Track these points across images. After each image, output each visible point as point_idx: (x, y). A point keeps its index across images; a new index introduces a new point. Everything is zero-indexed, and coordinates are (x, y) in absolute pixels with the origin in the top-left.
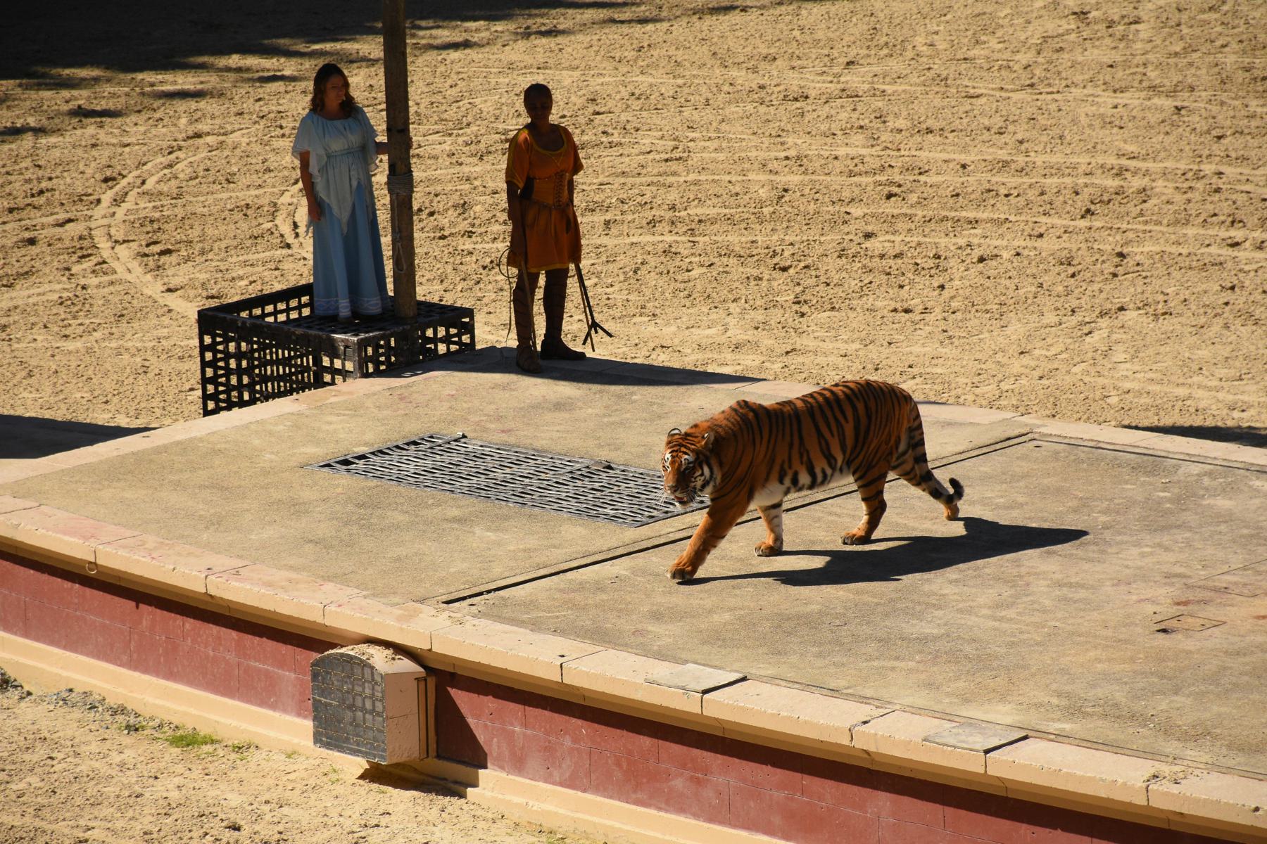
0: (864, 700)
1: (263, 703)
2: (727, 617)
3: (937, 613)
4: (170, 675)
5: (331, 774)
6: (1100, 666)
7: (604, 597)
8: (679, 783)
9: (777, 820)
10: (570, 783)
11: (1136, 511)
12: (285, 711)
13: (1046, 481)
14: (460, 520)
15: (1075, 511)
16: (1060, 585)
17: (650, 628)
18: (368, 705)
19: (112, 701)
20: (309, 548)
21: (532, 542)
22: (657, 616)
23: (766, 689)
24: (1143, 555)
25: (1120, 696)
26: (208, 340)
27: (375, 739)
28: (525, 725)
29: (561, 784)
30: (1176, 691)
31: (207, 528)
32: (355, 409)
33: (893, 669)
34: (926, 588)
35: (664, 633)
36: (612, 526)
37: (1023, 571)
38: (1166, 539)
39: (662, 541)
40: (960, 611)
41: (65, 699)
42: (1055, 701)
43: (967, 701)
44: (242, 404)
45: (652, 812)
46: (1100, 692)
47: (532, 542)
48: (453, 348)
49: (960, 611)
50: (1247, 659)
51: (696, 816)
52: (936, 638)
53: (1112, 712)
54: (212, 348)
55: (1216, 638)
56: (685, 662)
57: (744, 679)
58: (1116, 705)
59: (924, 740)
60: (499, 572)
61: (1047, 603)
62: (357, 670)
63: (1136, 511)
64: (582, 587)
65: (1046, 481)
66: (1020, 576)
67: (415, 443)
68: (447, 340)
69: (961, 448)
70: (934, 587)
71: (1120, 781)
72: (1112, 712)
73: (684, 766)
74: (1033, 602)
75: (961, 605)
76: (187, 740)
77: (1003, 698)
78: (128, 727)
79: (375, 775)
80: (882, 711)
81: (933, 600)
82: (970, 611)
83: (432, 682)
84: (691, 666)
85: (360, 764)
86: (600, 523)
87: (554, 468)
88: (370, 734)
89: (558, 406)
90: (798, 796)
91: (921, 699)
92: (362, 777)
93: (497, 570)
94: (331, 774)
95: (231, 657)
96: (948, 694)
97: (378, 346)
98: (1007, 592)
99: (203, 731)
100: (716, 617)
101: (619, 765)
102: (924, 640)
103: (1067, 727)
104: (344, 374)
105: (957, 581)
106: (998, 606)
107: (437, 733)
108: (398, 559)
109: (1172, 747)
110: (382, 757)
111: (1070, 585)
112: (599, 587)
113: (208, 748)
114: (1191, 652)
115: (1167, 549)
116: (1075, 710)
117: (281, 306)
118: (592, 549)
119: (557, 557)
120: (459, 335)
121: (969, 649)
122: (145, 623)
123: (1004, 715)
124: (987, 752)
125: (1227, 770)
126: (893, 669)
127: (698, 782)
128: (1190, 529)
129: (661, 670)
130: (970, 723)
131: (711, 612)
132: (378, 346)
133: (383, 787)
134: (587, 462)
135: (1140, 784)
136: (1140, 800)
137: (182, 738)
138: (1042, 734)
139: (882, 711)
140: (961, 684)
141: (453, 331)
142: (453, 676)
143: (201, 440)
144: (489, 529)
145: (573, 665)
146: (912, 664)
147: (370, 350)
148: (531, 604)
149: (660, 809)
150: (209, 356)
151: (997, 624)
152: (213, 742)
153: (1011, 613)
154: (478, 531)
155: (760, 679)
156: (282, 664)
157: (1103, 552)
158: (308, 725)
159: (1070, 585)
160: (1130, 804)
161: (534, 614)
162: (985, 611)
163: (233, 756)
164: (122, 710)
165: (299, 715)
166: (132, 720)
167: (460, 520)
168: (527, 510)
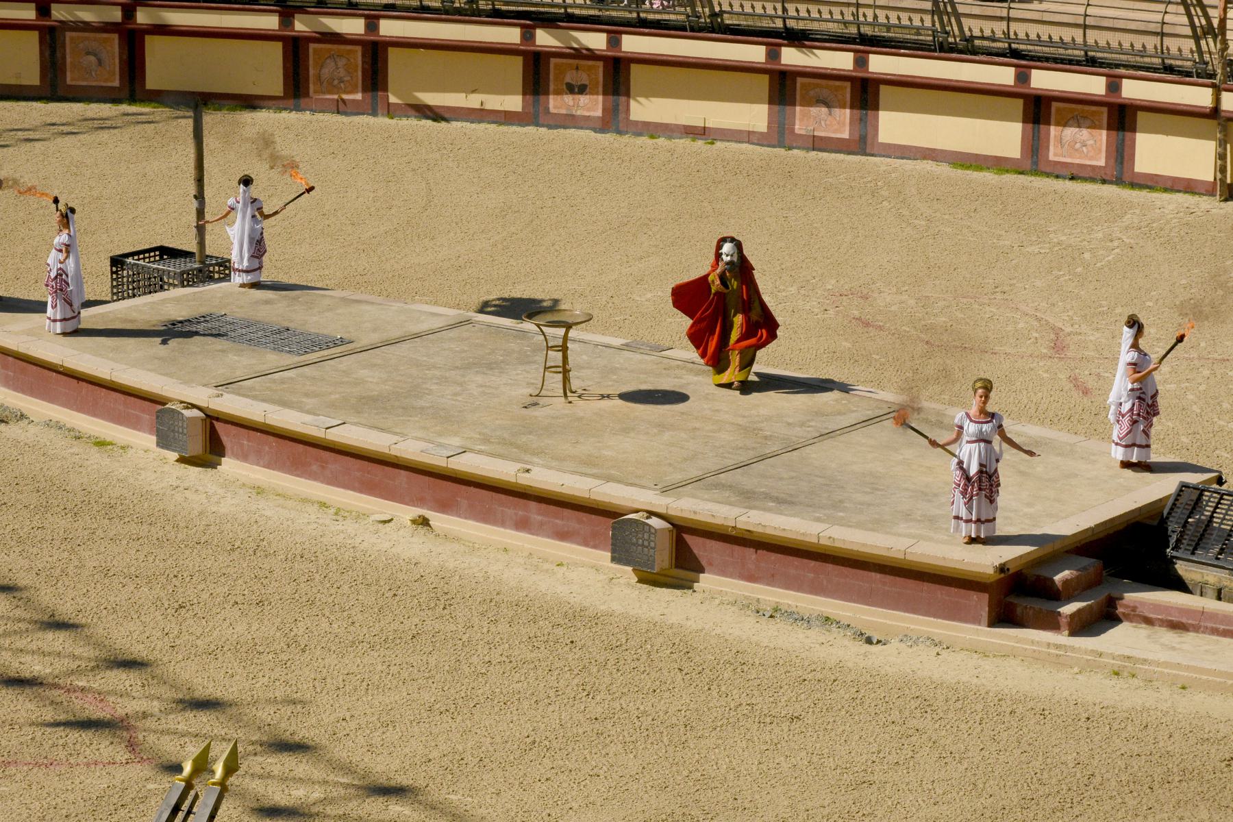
0: (396, 434)
1: (135, 428)
2: (337, 396)
3: (430, 397)
4: (95, 415)
5: (164, 460)
6: (497, 422)
7: (285, 386)
8: (314, 468)
9: (357, 485)
10: (268, 466)
11: (515, 355)
12: (145, 432)
13: (477, 341)
14: (223, 351)
15: (489, 354)
16: (482, 386)
17: (304, 400)
18: (181, 430)
19: (68, 426)
20: (156, 361)
21: (254, 361)
22: (307, 395)
23: (354, 428)
24: (517, 374)
25: (506, 435)
26: (114, 269)
27: (183, 445)
28: (249, 441)
29: (263, 467)
30: (530, 433)
31: (112, 351)
32: (177, 300)
33: (409, 421)
34: (424, 386)
35: (310, 402)
36: (288, 355)
37: (466, 379)
38: (528, 367)
39: (310, 362)
40: (438, 396)
41: (49, 424)
42: (478, 436)
43: (441, 435)
44: (129, 297)
45: (303, 480)
46: (498, 433)
47: (254, 361)
48: (222, 276)
49: (438, 396)
50: (561, 421)
51: (322, 482)
52: (428, 408)
53: (503, 442)
54: (116, 273)
55: (547, 411)
56: (319, 415)
57: (344, 423)
58: (504, 439)
59: (422, 452)
60: (239, 374)
61: (475, 393)
62: (176, 415)
63: (515, 355)
64: (274, 381)
65: (477, 341)
66: (464, 382)
67: (204, 317)
68: (219, 272)
69: (441, 326)
70: (428, 386)
71: (505, 471)
72: (503, 442)
73: (317, 460)
74: (470, 394)
75: (439, 394)
76: (101, 444)
77: (456, 434)
78: (75, 437)
79: (182, 460)
80: (403, 439)
81: (427, 392)
82: (442, 396)
83: (208, 421)
84: (321, 417)
85: (175, 456)
86: (283, 354)
87: (264, 330)
88: (181, 443)
89: (267, 302)
90: (366, 475)
91: (420, 434)
92: (177, 461)
93: (238, 373)
94: (164, 460)
95: (121, 408)
96: (432, 433)
97: (189, 274)
98: (459, 389)
99: (108, 439)
100: (333, 397)
101: (288, 458)
102: (422, 408)
103: (483, 448)
104: (175, 286)
105: (437, 383)
106: (456, 394)
107: (210, 443)
108: (195, 367)
109: (527, 457)
110: (186, 453)
111: (485, 386)
112: (283, 382)
113: (109, 447)
114: (536, 417)
115: (528, 372)
116: (486, 440)
117: (147, 255)
118: (279, 365)
119: (264, 368)
120: (224, 270)
121: (442, 413)
122: (84, 392)
123: (456, 441)
124: (448, 457)
125: (550, 468)
126: (409, 421)
127: (323, 467)
128: (538, 364)
129: (308, 418)
130: (441, 445)
131: (330, 393)
132: (189, 274)
133: (186, 466)
134: (278, 327)
135: (513, 473)
136: (513, 480)
137: (99, 442)
138: (472, 451)
139: (403, 439)
140: (438, 428)
141: (221, 268)
142: (217, 419)
143: (110, 312)
144: (235, 355)
145: (270, 415)
146: (416, 419)
147: (185, 276)
148: (252, 389)
149: (306, 478)
150: (114, 276)
151: (454, 402)
152: (112, 444)
153: (460, 398)
154: (230, 356)
155: (352, 424)
156: (143, 411)
157: (501, 372)
158: (154, 438)
159: (485, 386)
160: (509, 481)
161: (254, 393)
162: (449, 397)
163: (121, 451)
164: (72, 430)
165: (150, 434)
166: (77, 434)
167: (223, 351)
168: (252, 347)
